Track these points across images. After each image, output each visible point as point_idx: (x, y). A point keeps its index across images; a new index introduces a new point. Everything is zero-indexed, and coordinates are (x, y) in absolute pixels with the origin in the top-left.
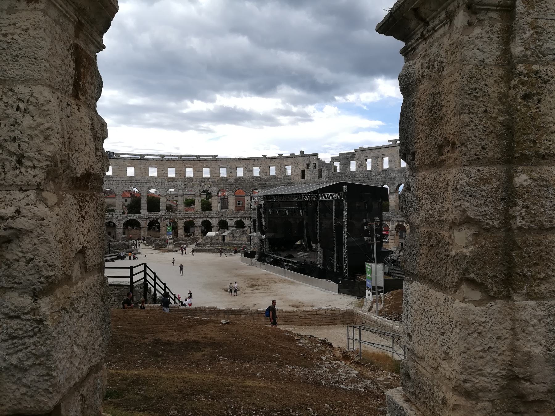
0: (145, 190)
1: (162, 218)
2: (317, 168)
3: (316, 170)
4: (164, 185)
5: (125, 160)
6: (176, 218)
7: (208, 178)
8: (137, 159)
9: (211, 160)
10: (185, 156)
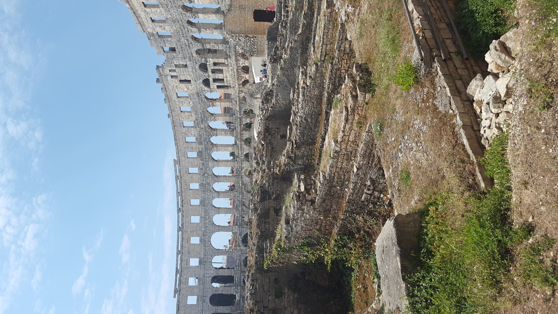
0: (213, 228)
2: (174, 68)
3: (177, 70)
4: (208, 210)
5: (184, 246)
7: (200, 169)
10: (177, 190)
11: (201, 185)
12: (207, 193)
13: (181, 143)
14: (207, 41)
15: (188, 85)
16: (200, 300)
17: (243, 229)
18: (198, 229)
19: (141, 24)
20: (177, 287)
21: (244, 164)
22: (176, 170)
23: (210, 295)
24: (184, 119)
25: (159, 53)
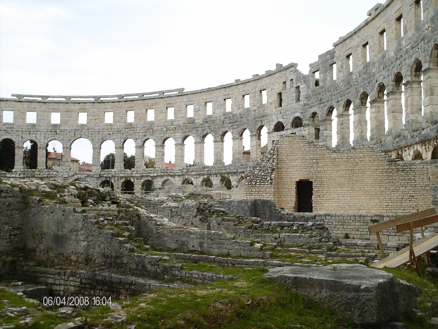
0: (97, 141)
1: (115, 177)
5: (75, 104)
7: (172, 121)
10: (146, 94)
11: (152, 123)
15: (277, 104)
16: (8, 126)
20: (25, 98)
23: (14, 139)
25: (311, 65)
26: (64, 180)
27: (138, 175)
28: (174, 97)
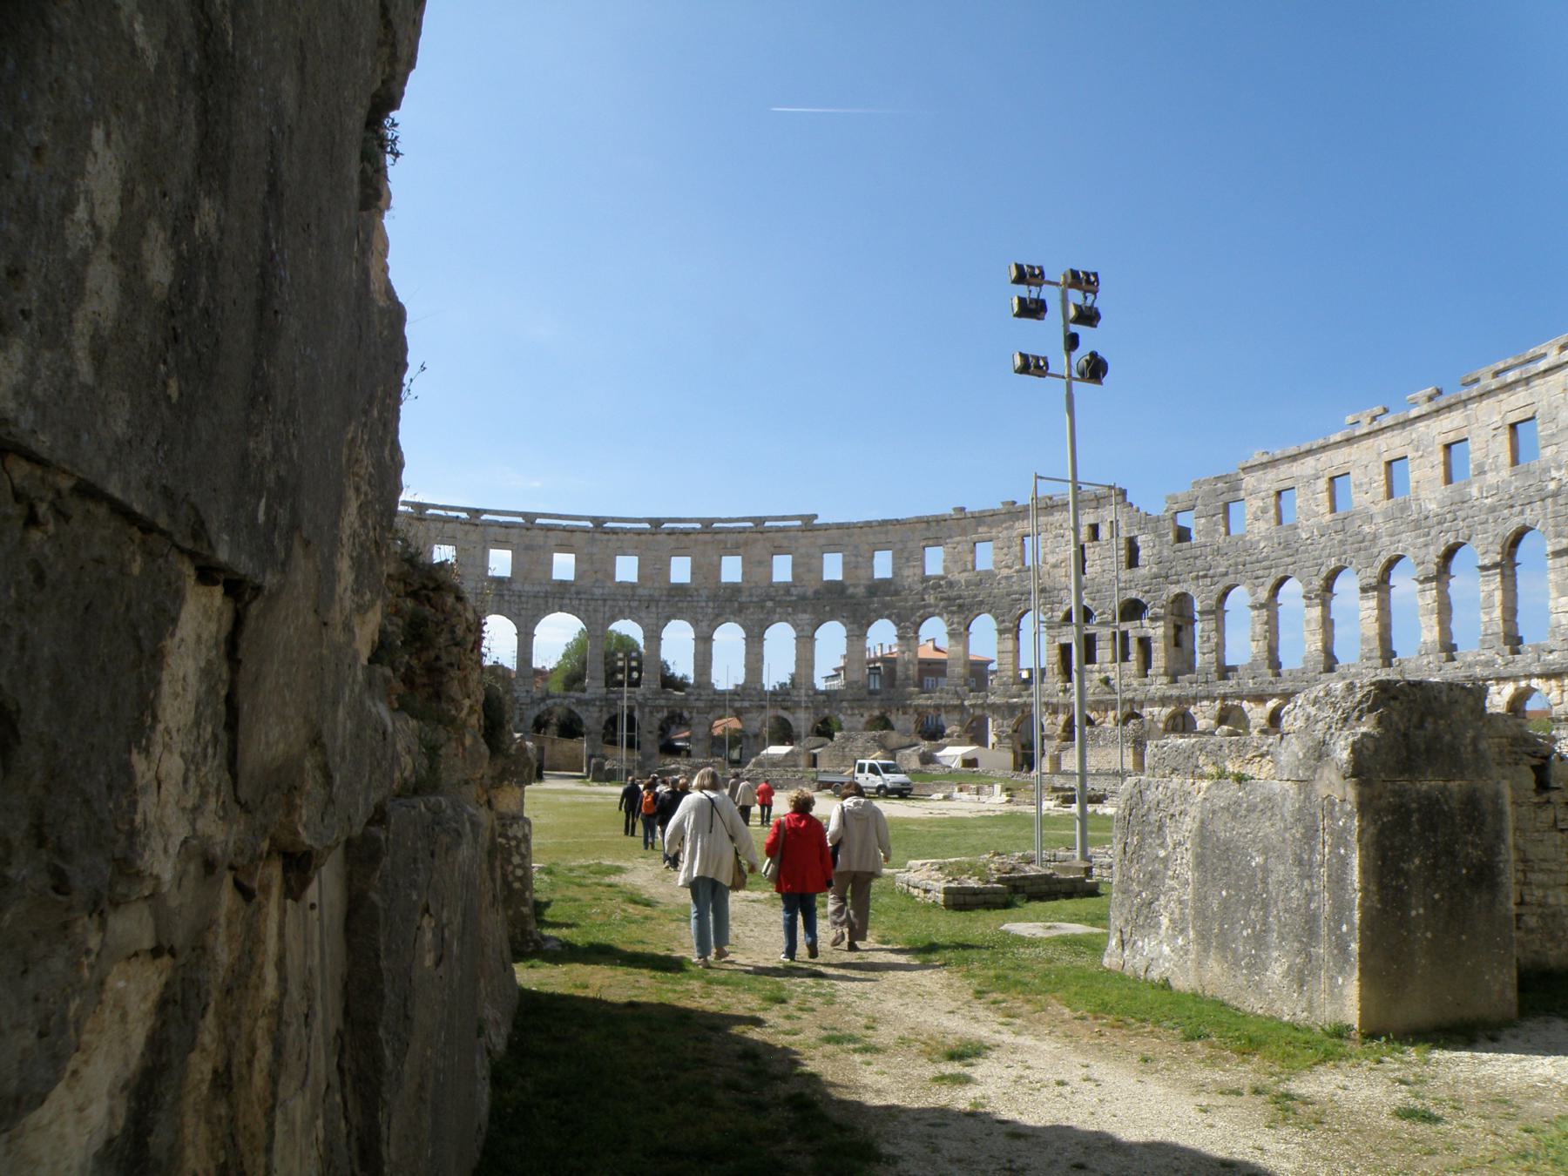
0: (600, 621)
5: (550, 533)
6: (688, 708)
7: (786, 588)
8: (584, 530)
9: (798, 529)
11: (734, 588)
12: (711, 604)
13: (872, 539)
14: (1220, 623)
17: (597, 709)
18: (599, 576)
19: (1273, 463)
20: (430, 511)
21: (807, 716)
22: (784, 518)
24: (951, 550)
26: (521, 709)
27: (700, 704)
28: (792, 533)
